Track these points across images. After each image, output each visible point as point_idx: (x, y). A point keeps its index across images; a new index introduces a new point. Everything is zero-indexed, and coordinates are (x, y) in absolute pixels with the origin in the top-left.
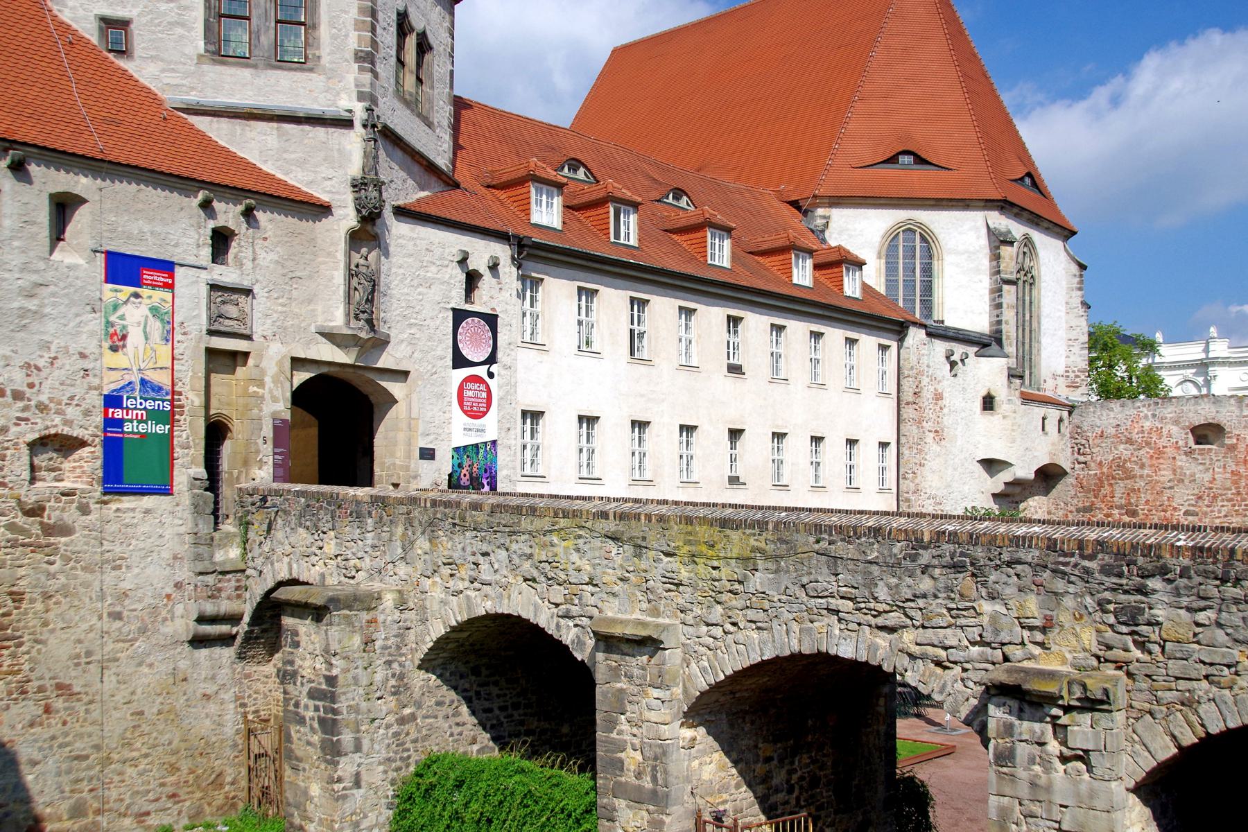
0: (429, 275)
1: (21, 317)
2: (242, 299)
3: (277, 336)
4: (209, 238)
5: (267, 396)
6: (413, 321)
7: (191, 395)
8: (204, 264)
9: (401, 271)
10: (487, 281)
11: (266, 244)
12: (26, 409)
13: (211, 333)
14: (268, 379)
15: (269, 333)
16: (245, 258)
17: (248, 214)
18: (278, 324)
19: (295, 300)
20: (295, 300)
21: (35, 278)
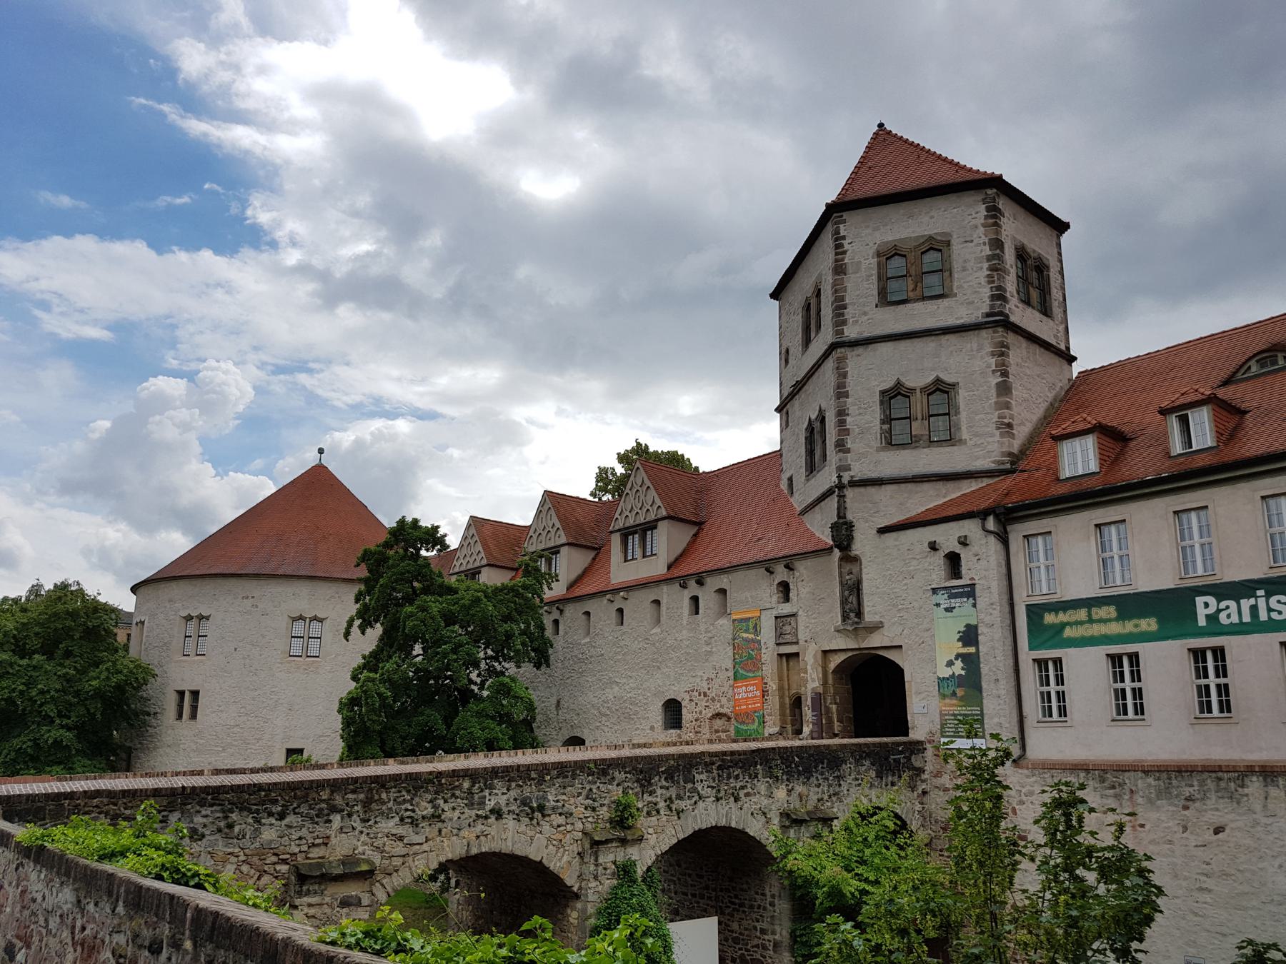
0: (912, 568)
1: (706, 655)
2: (792, 620)
5: (809, 678)
6: (900, 607)
7: (771, 683)
8: (773, 606)
9: (889, 572)
10: (965, 555)
11: (803, 583)
12: (707, 701)
13: (778, 644)
14: (809, 667)
15: (808, 638)
17: (789, 567)
21: (710, 635)
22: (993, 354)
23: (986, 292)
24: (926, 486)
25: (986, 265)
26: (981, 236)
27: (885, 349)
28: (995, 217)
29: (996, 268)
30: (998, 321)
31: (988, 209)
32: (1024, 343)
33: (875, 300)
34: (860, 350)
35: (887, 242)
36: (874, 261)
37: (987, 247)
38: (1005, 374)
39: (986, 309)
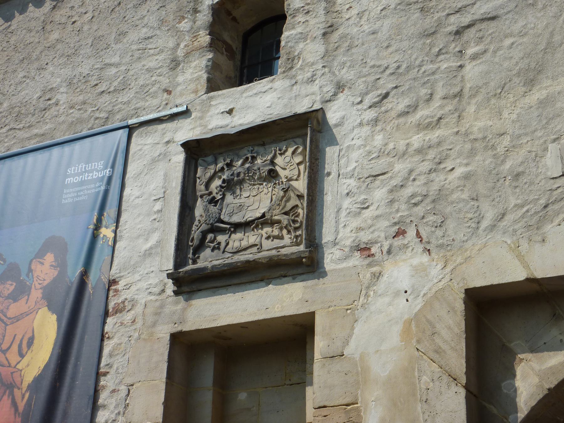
3: (411, 233)
4: (203, 33)
16: (303, 37)
18: (408, 191)
19: (475, 91)
20: (475, 91)
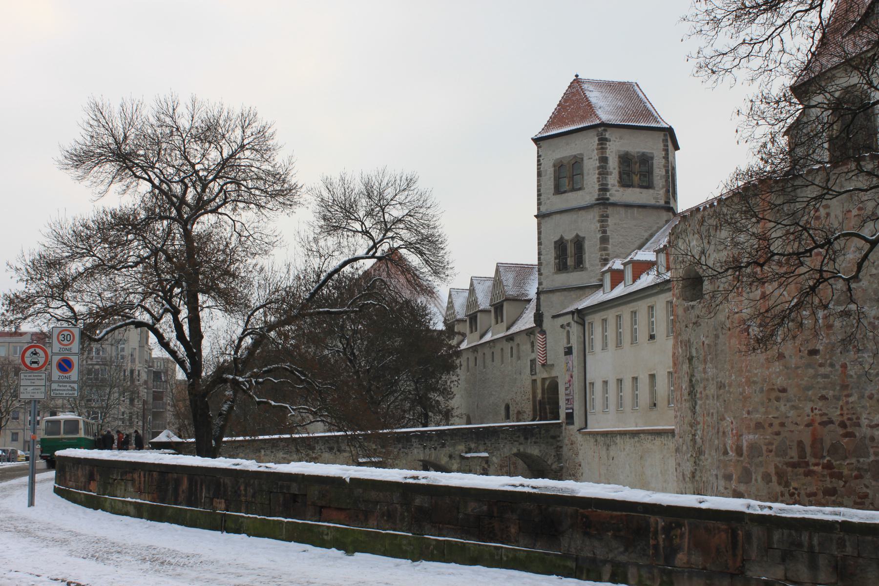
13: (532, 375)
22: (599, 221)
23: (597, 187)
24: (572, 293)
25: (597, 172)
26: (595, 155)
27: (557, 217)
28: (601, 144)
29: (603, 171)
30: (603, 203)
31: (599, 140)
32: (622, 210)
33: (552, 191)
34: (547, 219)
35: (558, 159)
36: (552, 169)
37: (598, 162)
38: (604, 232)
39: (596, 197)
